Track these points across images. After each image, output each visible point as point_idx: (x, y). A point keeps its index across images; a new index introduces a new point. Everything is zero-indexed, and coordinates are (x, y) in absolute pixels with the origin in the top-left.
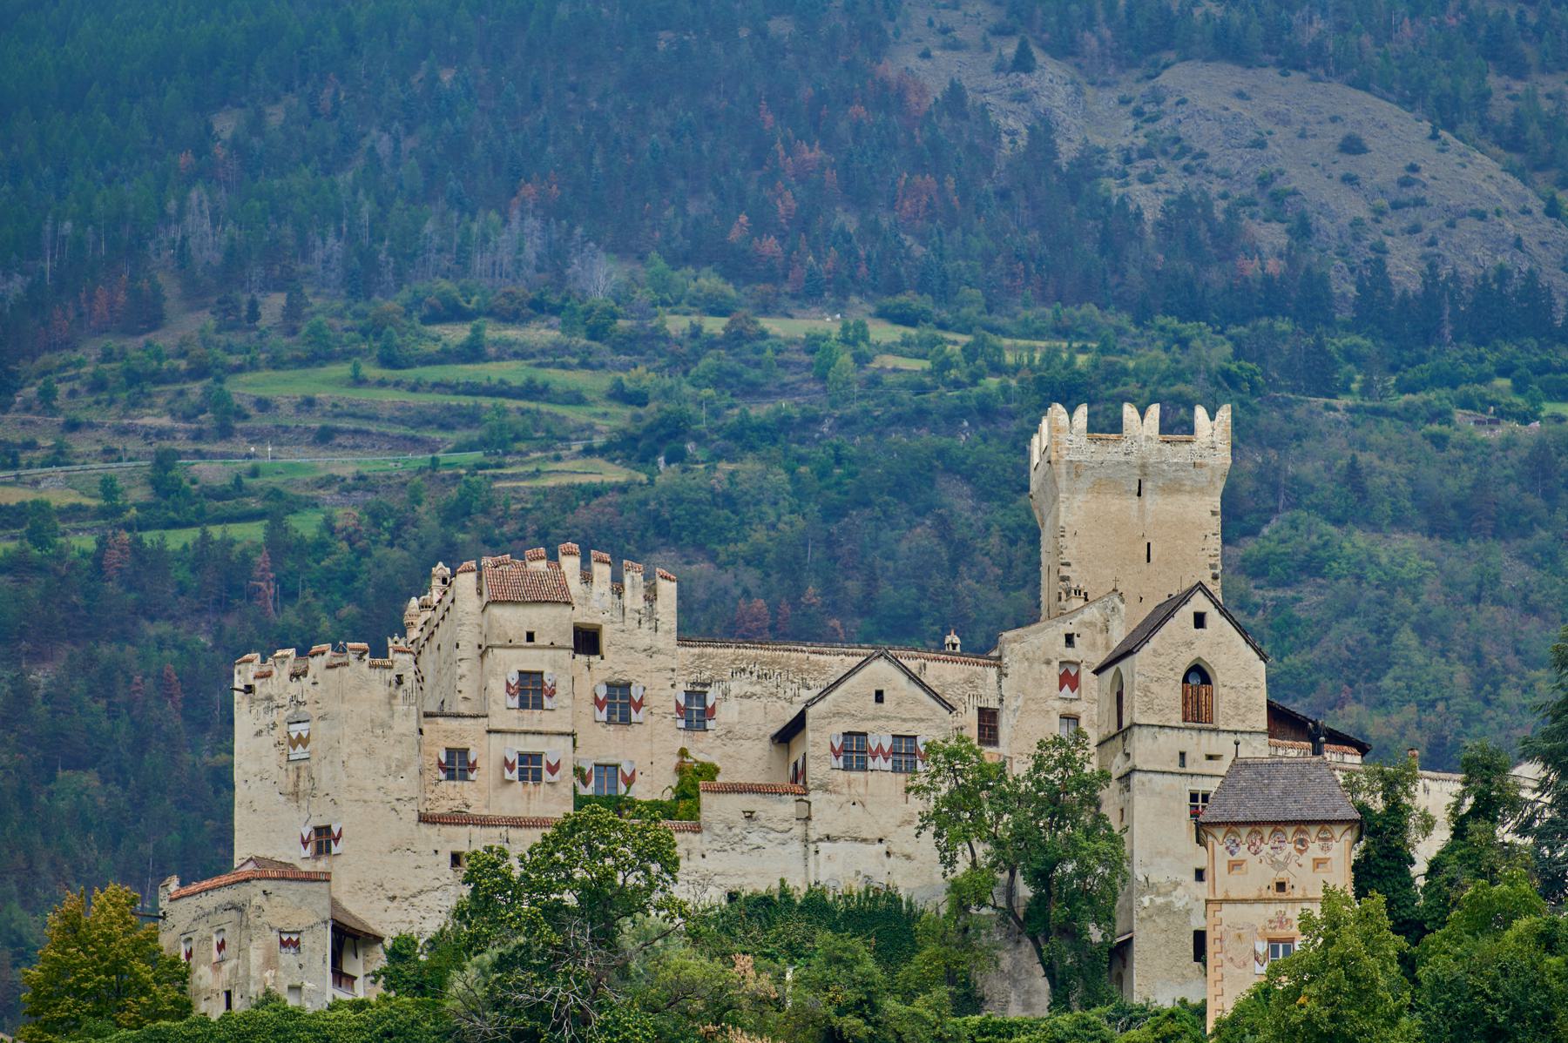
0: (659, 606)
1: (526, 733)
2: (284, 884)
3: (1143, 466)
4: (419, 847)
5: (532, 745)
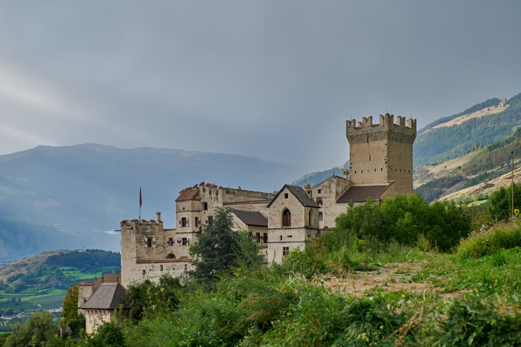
0: (219, 196)
1: (183, 233)
2: (84, 287)
3: (367, 134)
4: (136, 269)
5: (184, 236)
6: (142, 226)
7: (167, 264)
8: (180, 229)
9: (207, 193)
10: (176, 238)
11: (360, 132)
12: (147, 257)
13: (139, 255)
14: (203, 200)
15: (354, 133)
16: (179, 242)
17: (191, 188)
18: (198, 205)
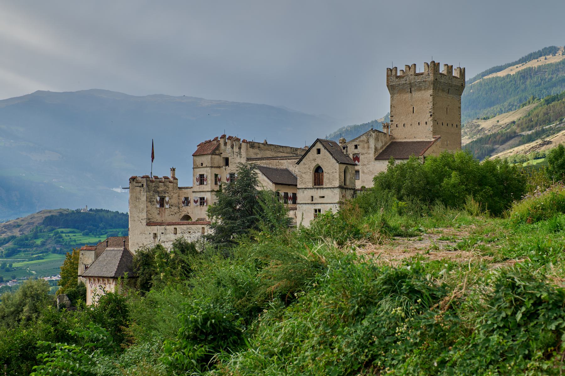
4: (146, 232)
6: (154, 184)
7: (182, 226)
8: (197, 188)
9: (229, 146)
10: (193, 197)
11: (403, 81)
12: (158, 219)
13: (150, 216)
14: (224, 155)
15: (395, 82)
16: (196, 202)
17: (210, 141)
18: (218, 160)
